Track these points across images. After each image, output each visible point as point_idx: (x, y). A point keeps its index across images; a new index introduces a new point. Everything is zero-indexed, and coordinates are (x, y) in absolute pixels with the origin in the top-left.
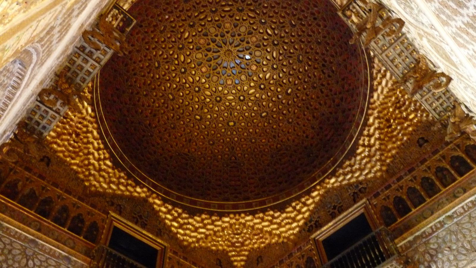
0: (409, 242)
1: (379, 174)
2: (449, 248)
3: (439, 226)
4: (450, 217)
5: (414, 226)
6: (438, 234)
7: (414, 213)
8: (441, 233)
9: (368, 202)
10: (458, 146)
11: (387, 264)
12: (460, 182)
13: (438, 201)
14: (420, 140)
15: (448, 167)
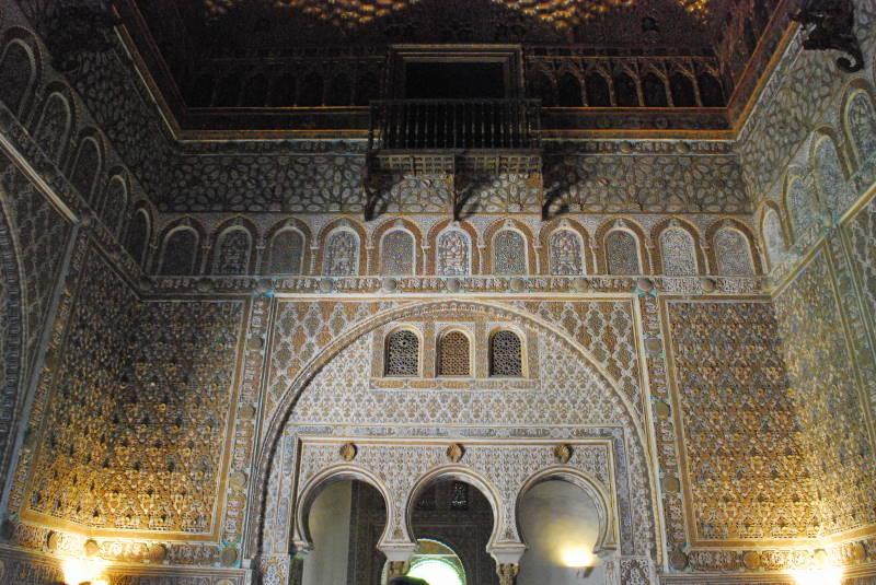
0: (556, 143)
1: (560, 24)
2: (608, 181)
3: (609, 148)
4: (631, 146)
5: (575, 127)
6: (601, 157)
7: (586, 110)
8: (607, 158)
9: (521, 53)
10: (695, 64)
11: (522, 153)
12: (670, 111)
13: (627, 117)
14: (648, 21)
15: (667, 83)
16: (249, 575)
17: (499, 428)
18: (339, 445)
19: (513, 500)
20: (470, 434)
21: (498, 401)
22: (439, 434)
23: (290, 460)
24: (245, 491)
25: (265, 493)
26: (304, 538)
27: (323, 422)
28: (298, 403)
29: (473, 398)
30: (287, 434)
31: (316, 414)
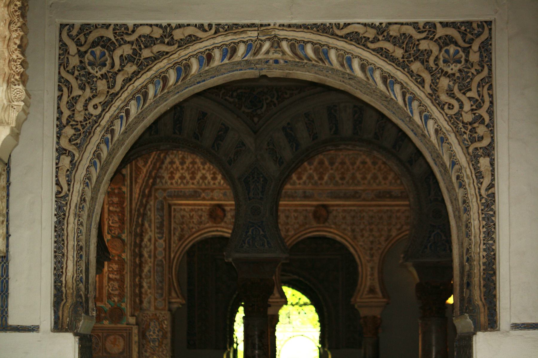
16: (135, 330)
17: (364, 190)
18: (208, 208)
19: (376, 259)
20: (335, 196)
21: (364, 163)
22: (305, 197)
23: (162, 224)
24: (124, 256)
25: (141, 256)
26: (180, 295)
27: (190, 186)
28: (164, 166)
29: (339, 160)
30: (156, 198)
31: (182, 178)
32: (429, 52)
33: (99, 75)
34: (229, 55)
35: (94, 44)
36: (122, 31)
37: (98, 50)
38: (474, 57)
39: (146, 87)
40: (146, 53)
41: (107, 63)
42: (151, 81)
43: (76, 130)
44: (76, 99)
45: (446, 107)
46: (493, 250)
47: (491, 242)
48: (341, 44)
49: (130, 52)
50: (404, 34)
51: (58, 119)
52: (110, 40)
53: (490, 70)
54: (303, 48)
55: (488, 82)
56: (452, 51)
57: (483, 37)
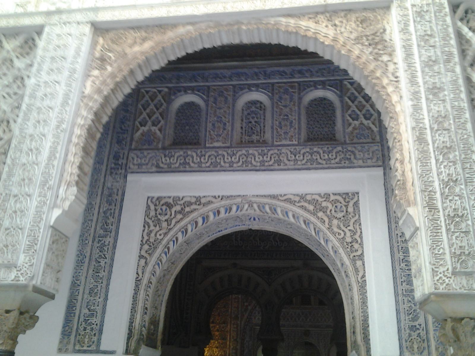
32: (327, 208)
33: (164, 219)
34: (228, 211)
35: (163, 205)
36: (176, 200)
37: (164, 208)
38: (350, 209)
39: (187, 225)
40: (187, 209)
41: (169, 213)
42: (190, 223)
43: (150, 246)
44: (151, 231)
45: (337, 235)
46: (367, 312)
47: (365, 308)
48: (282, 204)
49: (180, 209)
50: (314, 199)
51: (141, 241)
52: (170, 203)
53: (359, 216)
54: (264, 207)
55: (358, 222)
56: (339, 207)
57: (355, 199)
